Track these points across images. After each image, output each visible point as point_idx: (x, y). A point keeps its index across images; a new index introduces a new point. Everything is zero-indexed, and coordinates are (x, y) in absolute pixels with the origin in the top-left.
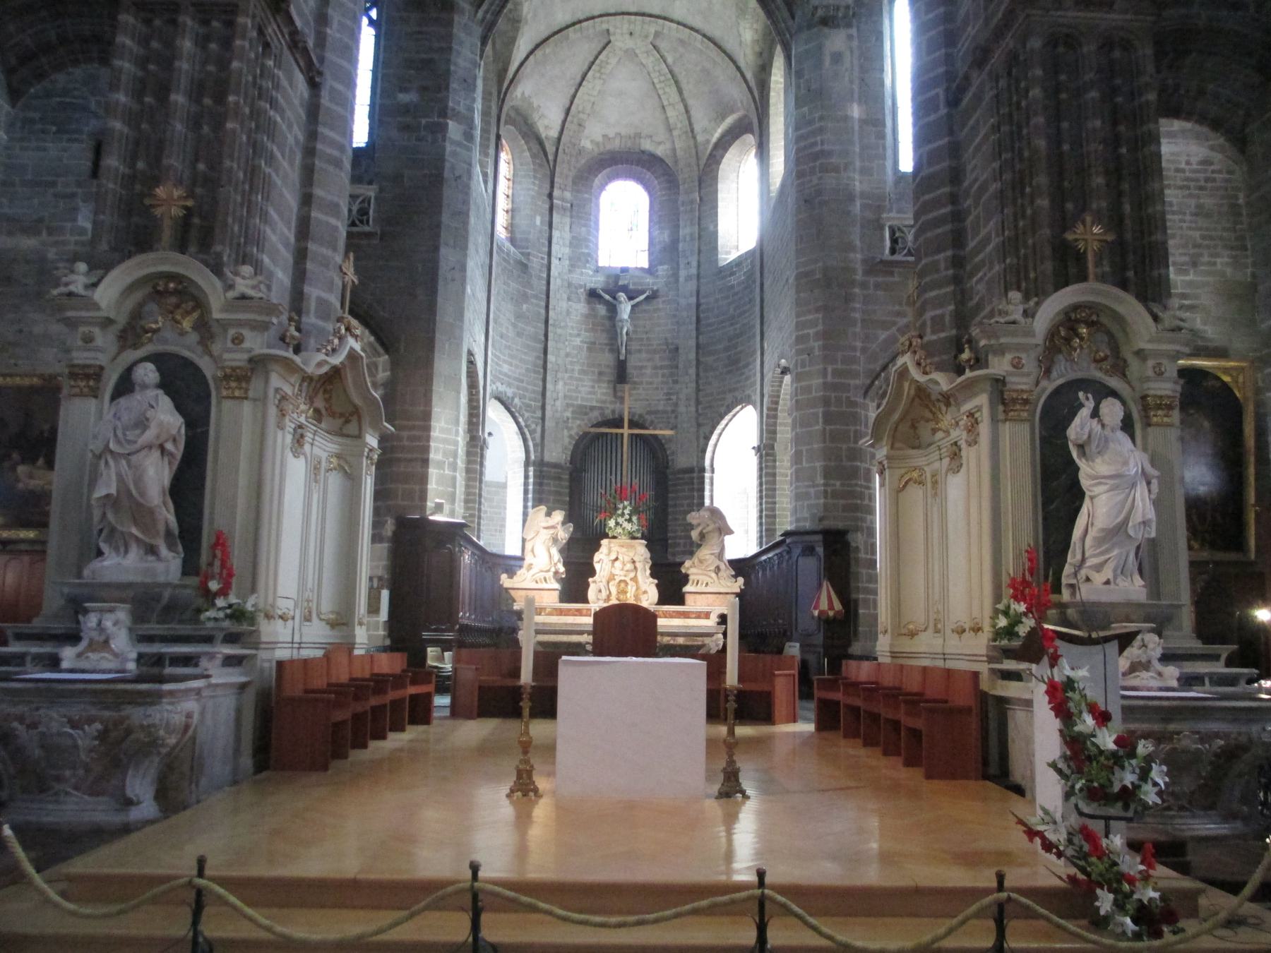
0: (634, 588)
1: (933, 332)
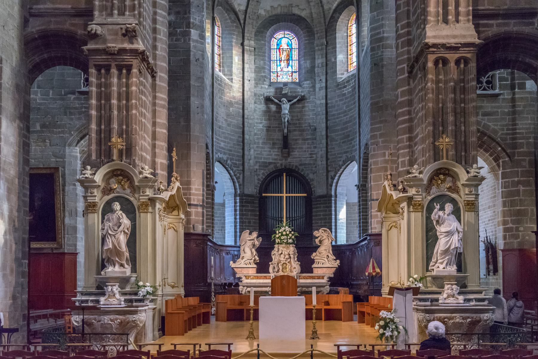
0: (290, 266)
1: (401, 167)
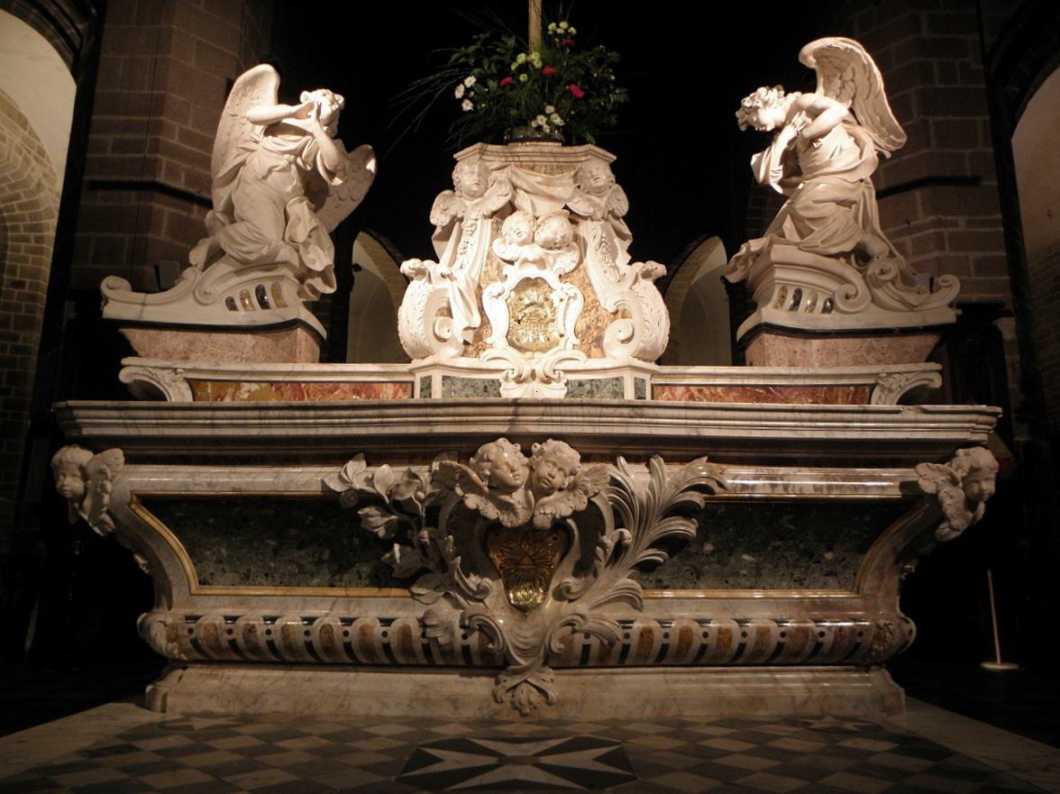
0: (577, 306)
